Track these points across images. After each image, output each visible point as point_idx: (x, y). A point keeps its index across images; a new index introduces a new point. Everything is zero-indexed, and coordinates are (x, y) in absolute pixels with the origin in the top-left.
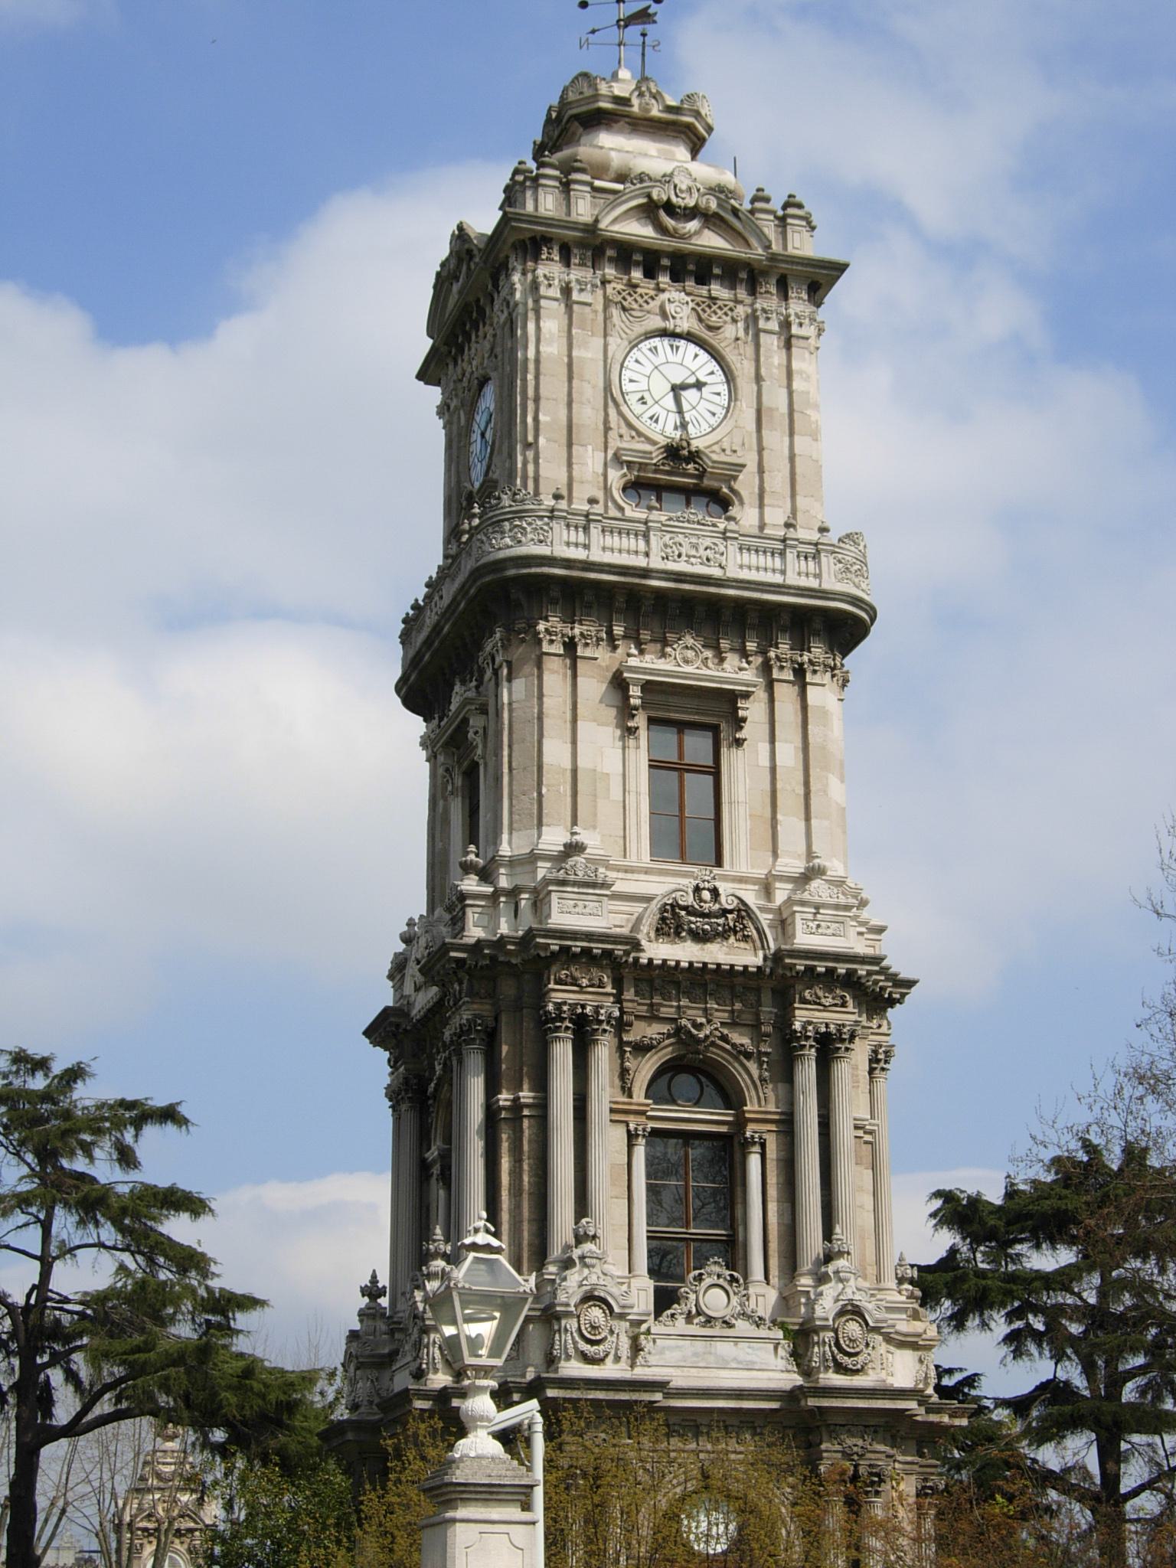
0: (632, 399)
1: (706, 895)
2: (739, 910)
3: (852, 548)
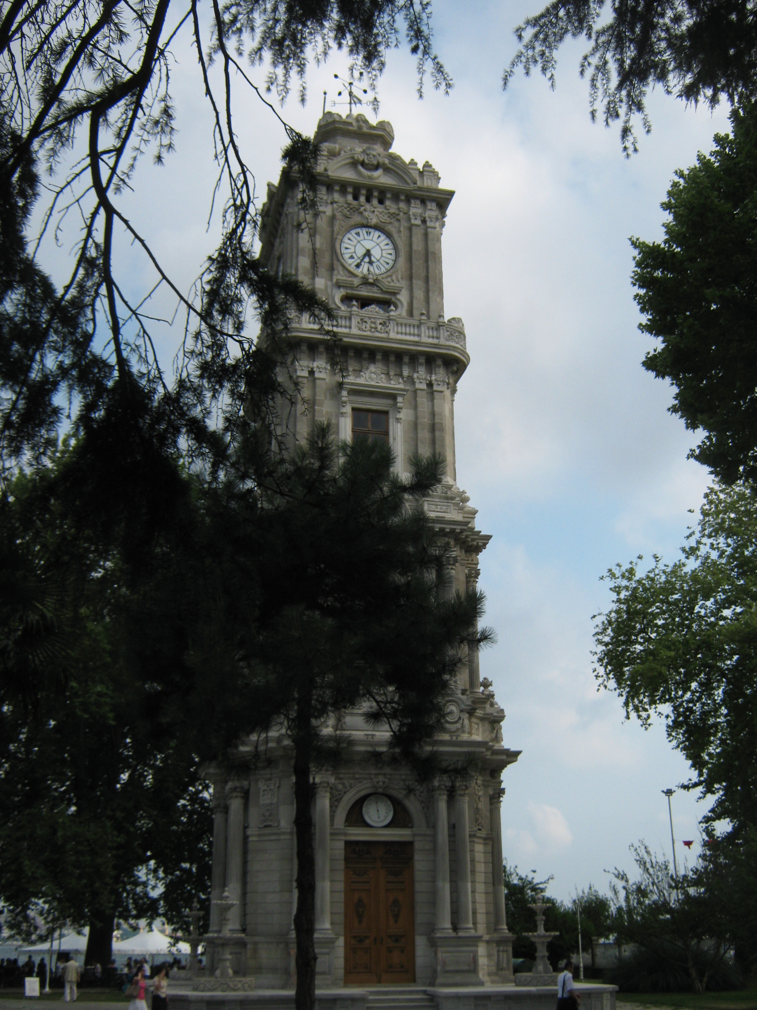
0: (346, 256)
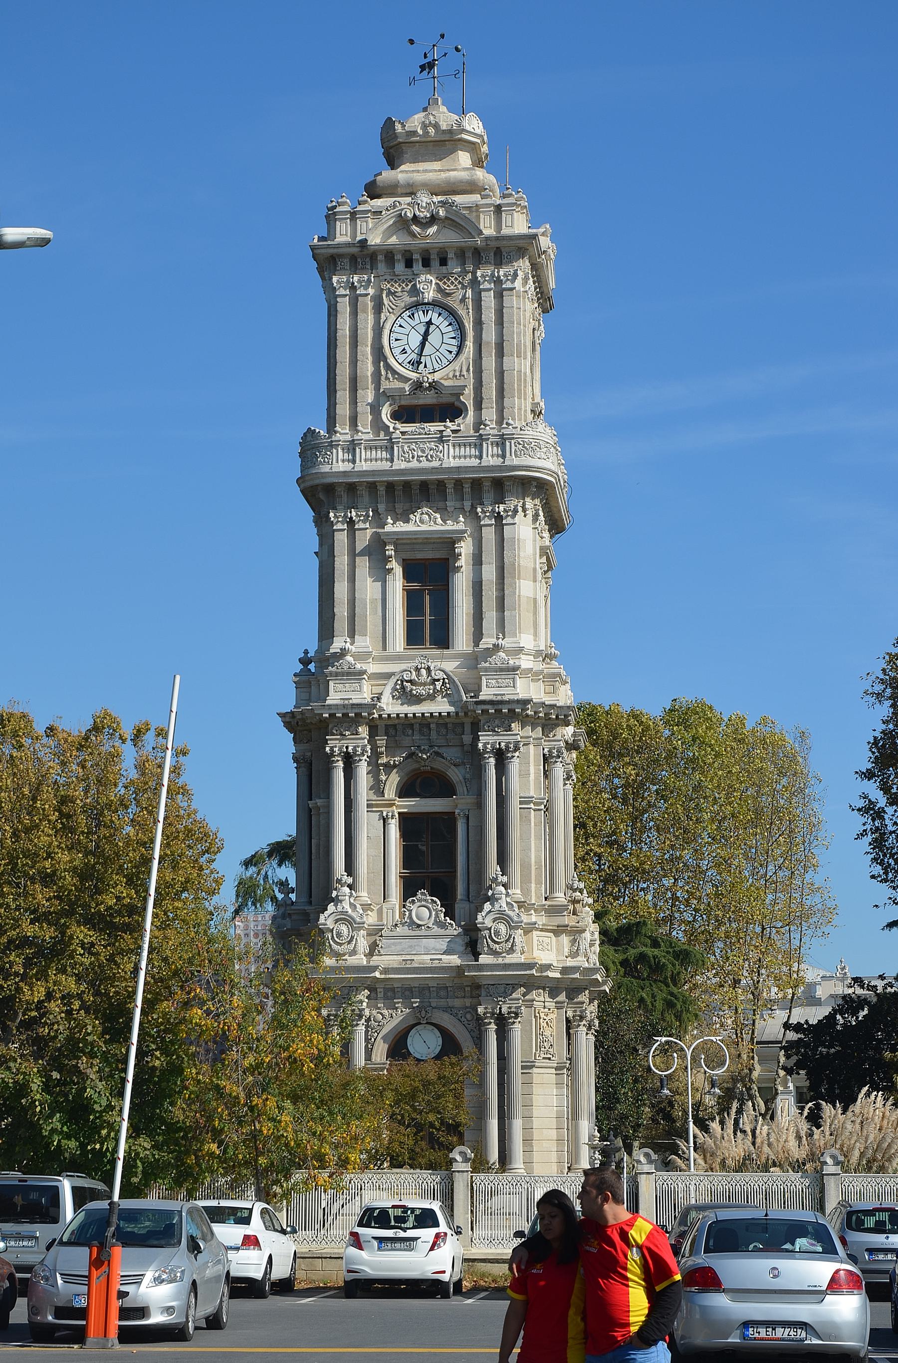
0: (397, 351)
1: (424, 672)
2: (444, 679)
3: (531, 433)
